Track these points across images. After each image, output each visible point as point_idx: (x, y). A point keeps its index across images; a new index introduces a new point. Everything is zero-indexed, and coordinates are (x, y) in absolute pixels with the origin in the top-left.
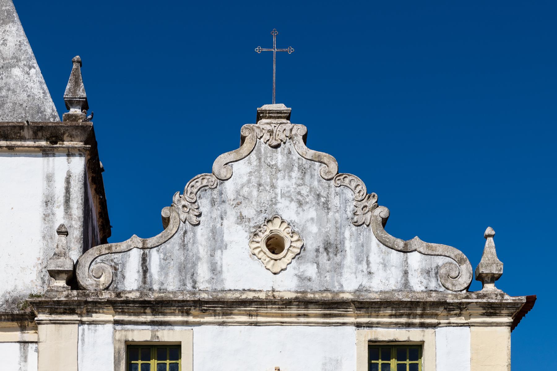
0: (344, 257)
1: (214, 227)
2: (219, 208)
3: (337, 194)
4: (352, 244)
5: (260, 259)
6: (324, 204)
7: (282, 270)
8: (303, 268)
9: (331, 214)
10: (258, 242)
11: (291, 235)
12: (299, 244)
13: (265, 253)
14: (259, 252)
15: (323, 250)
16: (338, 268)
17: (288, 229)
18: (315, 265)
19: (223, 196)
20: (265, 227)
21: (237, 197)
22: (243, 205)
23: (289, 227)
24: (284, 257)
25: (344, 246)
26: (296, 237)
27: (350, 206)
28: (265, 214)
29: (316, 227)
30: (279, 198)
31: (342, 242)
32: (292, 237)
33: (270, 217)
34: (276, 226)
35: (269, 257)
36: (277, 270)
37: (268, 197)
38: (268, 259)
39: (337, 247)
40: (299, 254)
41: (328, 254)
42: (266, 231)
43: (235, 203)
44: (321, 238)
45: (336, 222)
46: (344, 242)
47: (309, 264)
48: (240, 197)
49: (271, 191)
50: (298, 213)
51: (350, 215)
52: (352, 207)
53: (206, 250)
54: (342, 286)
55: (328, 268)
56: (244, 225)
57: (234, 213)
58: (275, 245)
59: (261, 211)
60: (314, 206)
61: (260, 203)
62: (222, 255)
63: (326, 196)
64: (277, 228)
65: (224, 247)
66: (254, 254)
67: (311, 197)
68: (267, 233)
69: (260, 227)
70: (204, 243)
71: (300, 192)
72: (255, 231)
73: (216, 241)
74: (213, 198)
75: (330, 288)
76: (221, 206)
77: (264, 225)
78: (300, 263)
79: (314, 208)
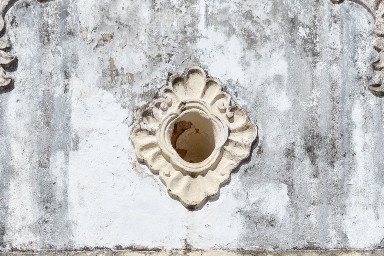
0: (351, 168)
1: (48, 96)
2: (60, 48)
3: (335, 19)
4: (368, 138)
5: (156, 173)
6: (305, 41)
7: (209, 198)
8: (256, 194)
9: (321, 66)
10: (151, 133)
11: (230, 114)
12: (247, 138)
13: (168, 159)
14: (155, 157)
15: (303, 152)
16: (336, 195)
17: (221, 100)
18: (285, 188)
19: (69, 18)
20: (168, 95)
21: (102, 23)
22: (117, 41)
23: (223, 96)
24: (214, 167)
25: (349, 142)
26: (240, 121)
27: (363, 49)
28: (169, 65)
29: (286, 99)
30: (201, 25)
31: (346, 134)
32: (231, 119)
33: (181, 72)
34: (193, 92)
35: (177, 168)
36: (196, 198)
37: (175, 24)
38: (175, 174)
39: (333, 146)
40: (247, 160)
41: (313, 162)
42: (170, 105)
43: (97, 36)
44: (299, 125)
45: (333, 86)
46: (350, 132)
47: (270, 186)
48: (109, 23)
49: (183, 9)
50: (245, 64)
51: (364, 68)
52: (369, 50)
53: (27, 151)
54: (345, 237)
55: (314, 194)
56: (119, 91)
57: (96, 62)
58: (191, 140)
59: (160, 56)
60: (282, 46)
61: (157, 38)
62: (67, 163)
63: (310, 25)
64: (197, 97)
65: (71, 143)
66: (143, 162)
67: (275, 26)
68: (174, 109)
69: (156, 96)
70: (23, 134)
71: (249, 12)
72: (146, 106)
73: (51, 130)
74: (45, 26)
75: (317, 241)
76: (65, 44)
77: (167, 91)
78: (249, 184)
79: (283, 51)
